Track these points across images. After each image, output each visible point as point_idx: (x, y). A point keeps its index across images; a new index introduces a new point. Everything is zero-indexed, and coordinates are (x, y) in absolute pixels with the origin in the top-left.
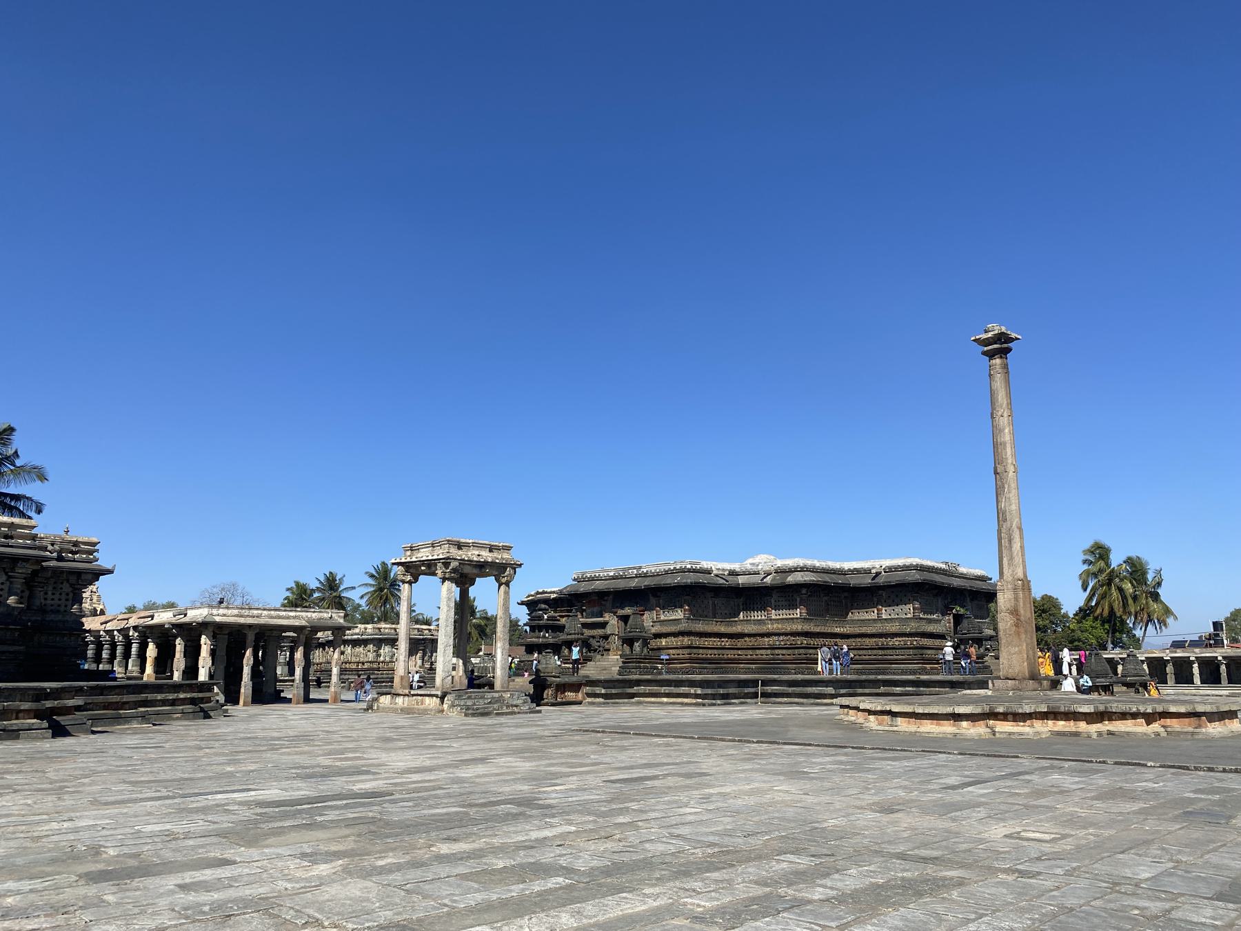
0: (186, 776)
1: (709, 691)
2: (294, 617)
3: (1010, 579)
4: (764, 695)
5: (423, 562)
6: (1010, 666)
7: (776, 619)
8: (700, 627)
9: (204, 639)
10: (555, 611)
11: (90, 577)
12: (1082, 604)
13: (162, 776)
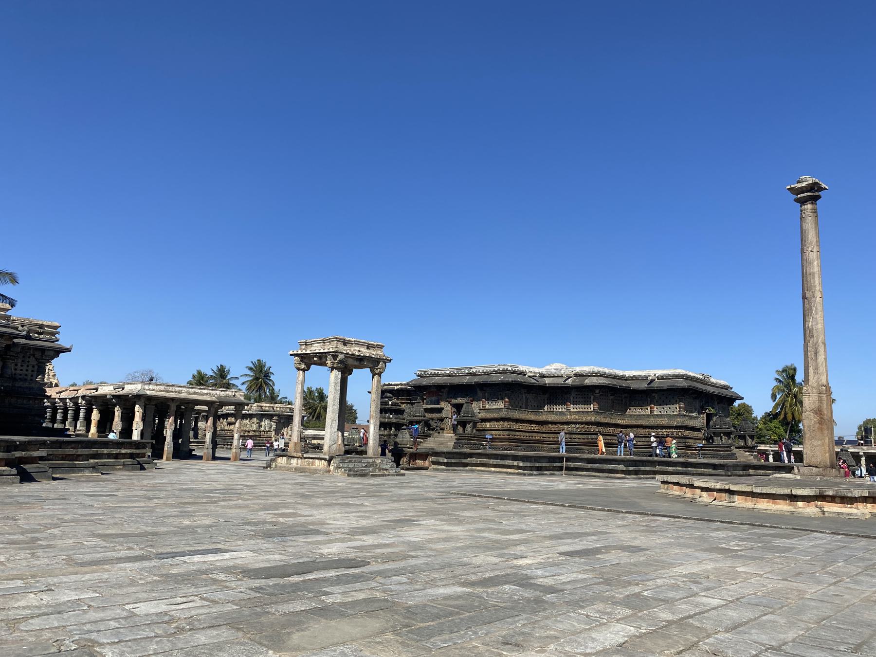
0: (149, 529)
1: (528, 464)
2: (207, 394)
3: (815, 385)
4: (568, 469)
5: (315, 354)
6: (813, 456)
7: (573, 411)
8: (516, 415)
9: (137, 407)
10: (398, 399)
11: (52, 353)
12: (769, 409)
13: (128, 530)
